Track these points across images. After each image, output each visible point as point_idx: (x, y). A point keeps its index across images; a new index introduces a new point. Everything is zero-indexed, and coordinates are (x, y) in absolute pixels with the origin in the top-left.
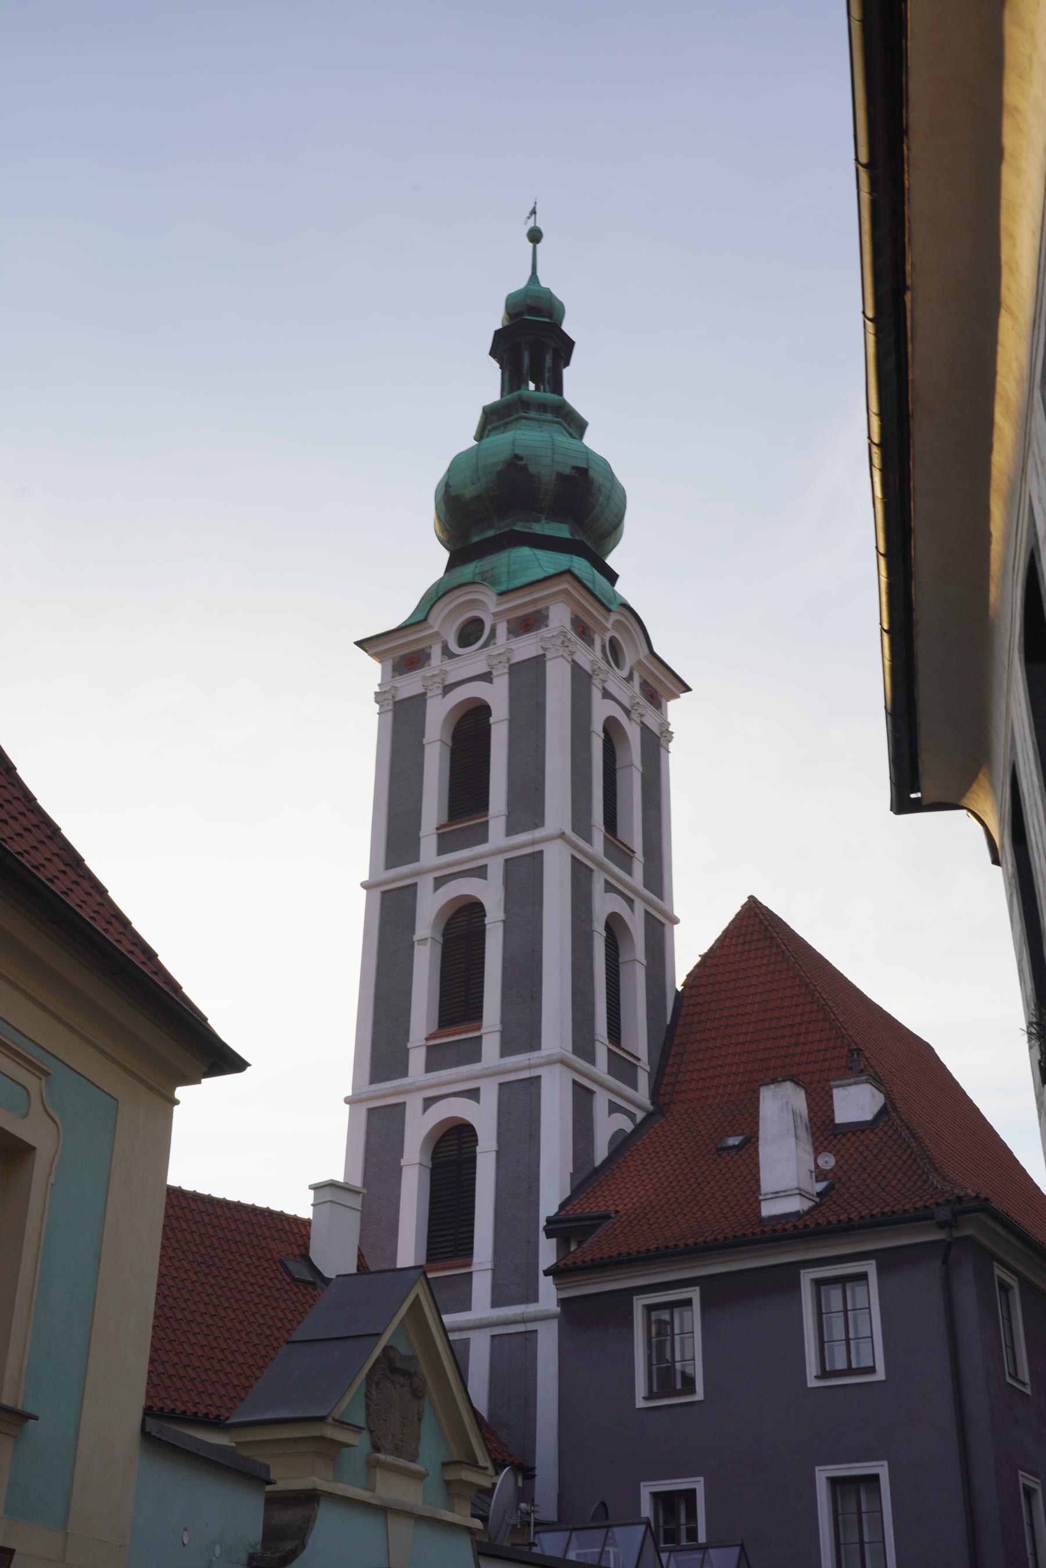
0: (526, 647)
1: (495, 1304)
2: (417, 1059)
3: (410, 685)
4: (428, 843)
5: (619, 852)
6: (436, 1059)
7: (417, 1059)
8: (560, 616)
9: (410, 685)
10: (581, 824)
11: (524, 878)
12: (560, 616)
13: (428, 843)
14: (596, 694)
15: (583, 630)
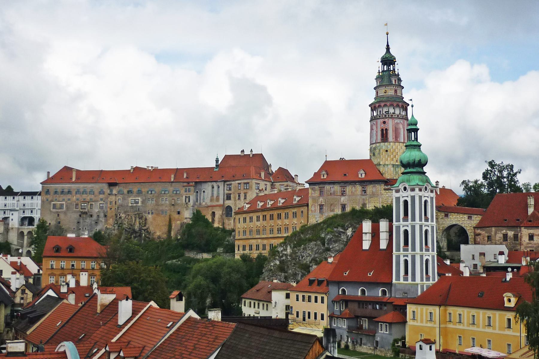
0: (413, 194)
1: (412, 281)
2: (401, 250)
3: (397, 195)
4: (401, 220)
5: (427, 220)
6: (404, 250)
7: (401, 250)
8: (417, 190)
9: (397, 195)
10: (421, 220)
11: (413, 227)
12: (417, 190)
13: (401, 220)
14: (423, 198)
15: (420, 190)
